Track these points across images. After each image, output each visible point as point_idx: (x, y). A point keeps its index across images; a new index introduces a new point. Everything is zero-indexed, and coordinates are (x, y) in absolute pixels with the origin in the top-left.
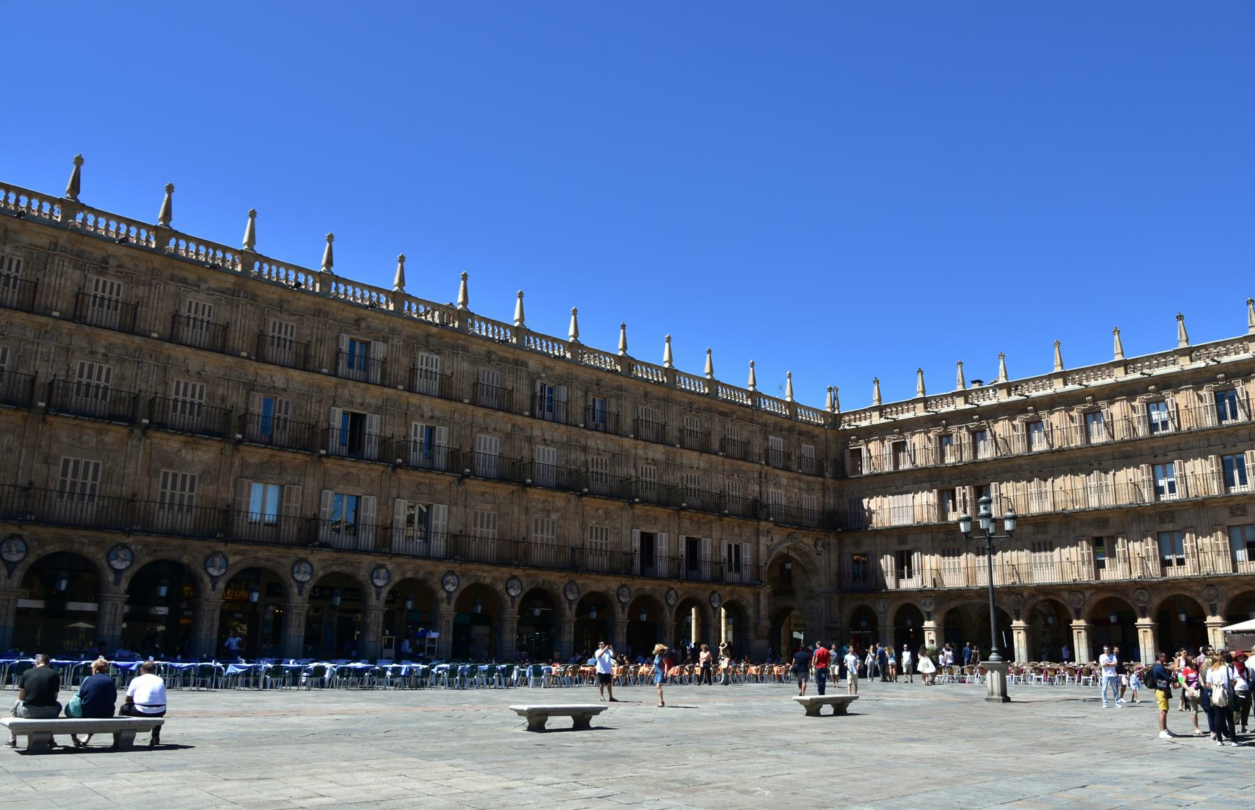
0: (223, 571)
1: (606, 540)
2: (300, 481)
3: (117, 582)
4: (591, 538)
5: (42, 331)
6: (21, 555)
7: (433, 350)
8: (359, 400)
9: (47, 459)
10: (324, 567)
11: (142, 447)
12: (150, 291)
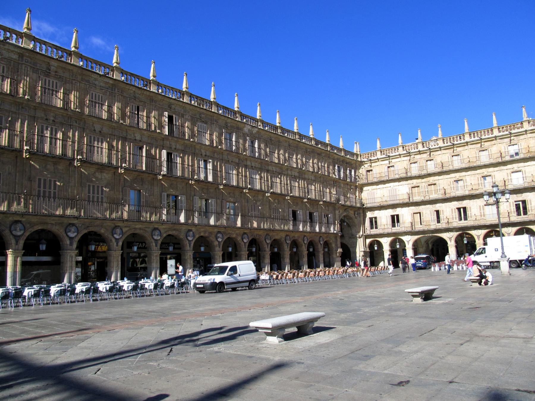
0: (121, 236)
1: (279, 214)
2: (151, 188)
3: (71, 244)
4: (273, 213)
5: (20, 107)
6: (22, 232)
7: (203, 122)
8: (174, 147)
9: (30, 178)
10: (166, 232)
11: (76, 171)
12: (72, 86)
